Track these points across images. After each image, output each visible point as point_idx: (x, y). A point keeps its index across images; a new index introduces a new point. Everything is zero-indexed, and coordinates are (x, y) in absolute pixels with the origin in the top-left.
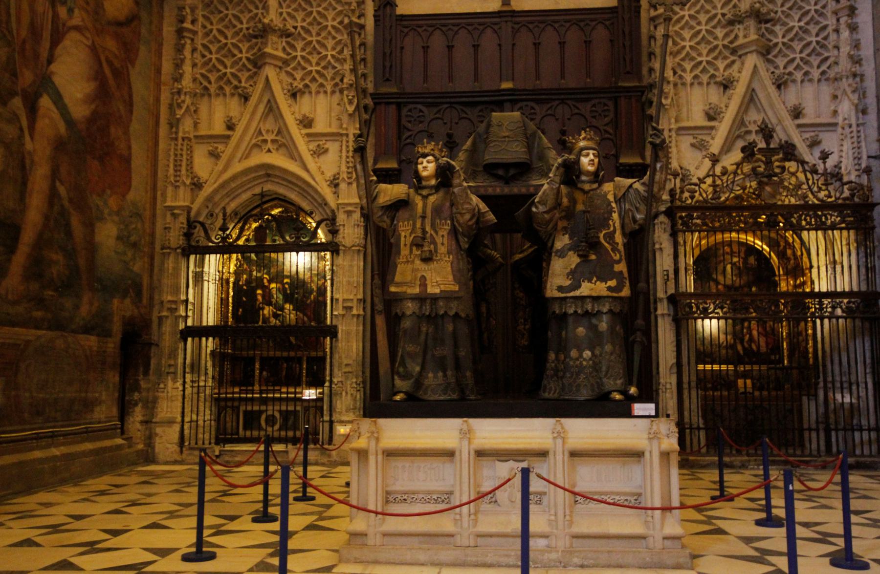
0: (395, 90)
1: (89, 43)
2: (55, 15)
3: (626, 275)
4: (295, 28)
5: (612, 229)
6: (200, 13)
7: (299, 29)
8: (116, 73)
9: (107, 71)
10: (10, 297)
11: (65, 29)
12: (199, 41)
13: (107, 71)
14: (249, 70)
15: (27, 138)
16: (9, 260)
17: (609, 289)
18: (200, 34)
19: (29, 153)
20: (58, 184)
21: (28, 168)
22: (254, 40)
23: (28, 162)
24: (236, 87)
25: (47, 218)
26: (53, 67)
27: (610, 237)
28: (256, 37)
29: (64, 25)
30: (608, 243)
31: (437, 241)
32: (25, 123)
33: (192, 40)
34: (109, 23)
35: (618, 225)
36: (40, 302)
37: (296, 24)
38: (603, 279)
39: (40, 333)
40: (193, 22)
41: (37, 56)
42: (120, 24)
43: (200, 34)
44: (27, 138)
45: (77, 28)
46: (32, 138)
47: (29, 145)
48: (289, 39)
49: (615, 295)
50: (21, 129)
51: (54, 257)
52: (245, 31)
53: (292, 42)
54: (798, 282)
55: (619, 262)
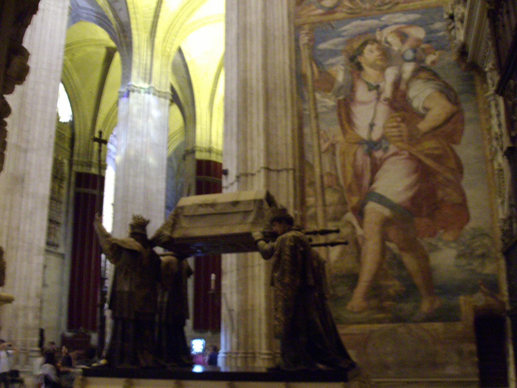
8: (438, 159)
9: (428, 162)
15: (358, 228)
26: (374, 186)
41: (360, 186)
44: (358, 228)
45: (395, 154)
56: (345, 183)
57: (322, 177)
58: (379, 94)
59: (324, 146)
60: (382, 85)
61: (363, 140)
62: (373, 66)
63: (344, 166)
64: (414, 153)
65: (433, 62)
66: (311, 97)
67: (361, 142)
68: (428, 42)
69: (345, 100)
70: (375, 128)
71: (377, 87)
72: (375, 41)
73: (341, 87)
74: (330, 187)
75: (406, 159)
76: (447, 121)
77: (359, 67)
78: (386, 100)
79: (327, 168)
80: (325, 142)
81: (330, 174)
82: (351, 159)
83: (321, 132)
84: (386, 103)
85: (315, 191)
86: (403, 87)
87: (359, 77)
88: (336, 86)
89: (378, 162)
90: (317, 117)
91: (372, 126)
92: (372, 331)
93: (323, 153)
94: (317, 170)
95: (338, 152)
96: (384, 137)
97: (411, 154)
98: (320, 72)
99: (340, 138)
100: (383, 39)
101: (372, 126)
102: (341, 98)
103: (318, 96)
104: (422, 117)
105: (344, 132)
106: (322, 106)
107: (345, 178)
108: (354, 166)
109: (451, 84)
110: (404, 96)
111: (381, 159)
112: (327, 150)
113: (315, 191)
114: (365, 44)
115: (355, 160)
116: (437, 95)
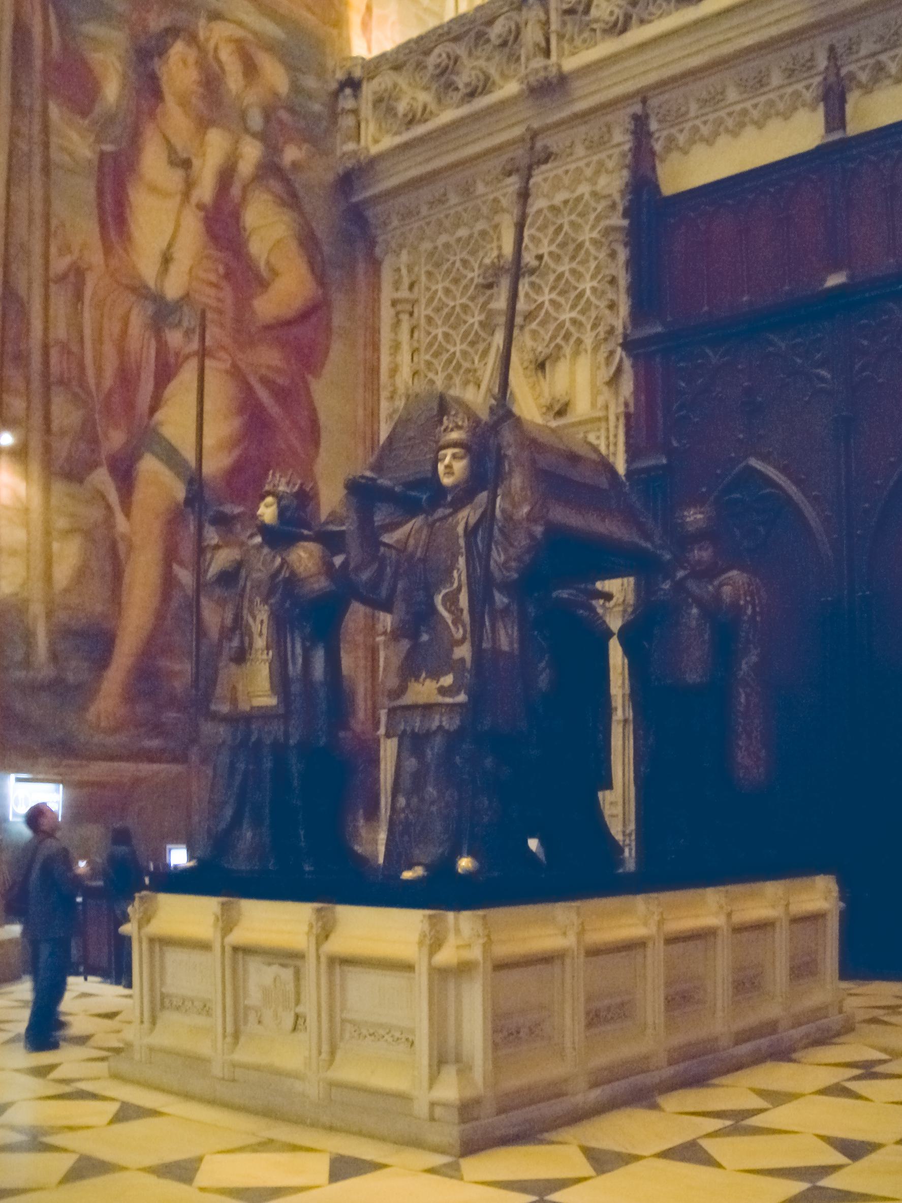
0: (659, 329)
1: (228, 365)
2: (162, 347)
3: (468, 664)
4: (540, 258)
5: (455, 585)
6: (422, 270)
7: (546, 257)
8: (282, 395)
10: (103, 724)
11: (180, 360)
12: (422, 311)
13: (263, 394)
14: (484, 340)
15: (120, 517)
16: (99, 678)
17: (442, 691)
18: (423, 301)
19: (124, 537)
20: (175, 567)
21: (122, 556)
22: (489, 292)
23: (122, 548)
24: (468, 371)
25: (160, 616)
26: (159, 416)
27: (452, 600)
28: (490, 286)
29: (177, 354)
30: (449, 611)
31: (253, 629)
32: (113, 497)
33: (411, 314)
34: (268, 328)
35: (464, 577)
36: (157, 729)
37: (540, 252)
38: (435, 675)
39: (155, 767)
40: (411, 286)
41: (130, 405)
42: (288, 323)
43: (423, 301)
44: (120, 517)
46: (127, 514)
47: (122, 524)
48: (533, 278)
49: (449, 700)
50: (109, 507)
51: (177, 667)
52: (475, 282)
53: (538, 281)
54: (466, 674)
55: (462, 641)
56: (98, 385)
57: (46, 348)
58: (189, 185)
59: (60, 265)
60: (196, 162)
61: (146, 287)
62: (184, 103)
63: (99, 340)
64: (242, 365)
65: (295, 165)
66: (38, 107)
67: (140, 291)
68: (292, 110)
69: (115, 156)
70: (173, 268)
71: (186, 164)
72: (193, 39)
73: (110, 119)
74: (61, 382)
75: (227, 372)
76: (305, 315)
77: (157, 94)
78: (200, 206)
79: (60, 331)
80: (61, 253)
81: (65, 349)
82: (116, 328)
83: (54, 222)
84: (202, 214)
85: (28, 382)
86: (236, 191)
87: (152, 115)
88: (98, 109)
89: (172, 360)
90: (46, 169)
91: (167, 260)
92: (137, 781)
93: (56, 282)
94: (37, 325)
95: (88, 293)
96: (186, 297)
97: (234, 365)
98: (65, 47)
99: (96, 257)
100: (211, 45)
101: (167, 260)
102: (108, 148)
103: (55, 111)
104: (264, 285)
105: (108, 250)
106: (63, 149)
107: (99, 370)
108: (122, 352)
109: (319, 234)
110: (236, 216)
111: (177, 354)
112: (63, 278)
113: (28, 382)
114: (173, 32)
115: (124, 332)
116: (293, 245)
